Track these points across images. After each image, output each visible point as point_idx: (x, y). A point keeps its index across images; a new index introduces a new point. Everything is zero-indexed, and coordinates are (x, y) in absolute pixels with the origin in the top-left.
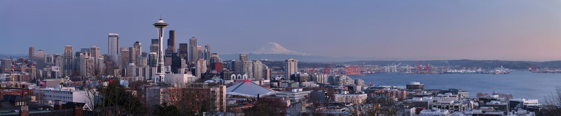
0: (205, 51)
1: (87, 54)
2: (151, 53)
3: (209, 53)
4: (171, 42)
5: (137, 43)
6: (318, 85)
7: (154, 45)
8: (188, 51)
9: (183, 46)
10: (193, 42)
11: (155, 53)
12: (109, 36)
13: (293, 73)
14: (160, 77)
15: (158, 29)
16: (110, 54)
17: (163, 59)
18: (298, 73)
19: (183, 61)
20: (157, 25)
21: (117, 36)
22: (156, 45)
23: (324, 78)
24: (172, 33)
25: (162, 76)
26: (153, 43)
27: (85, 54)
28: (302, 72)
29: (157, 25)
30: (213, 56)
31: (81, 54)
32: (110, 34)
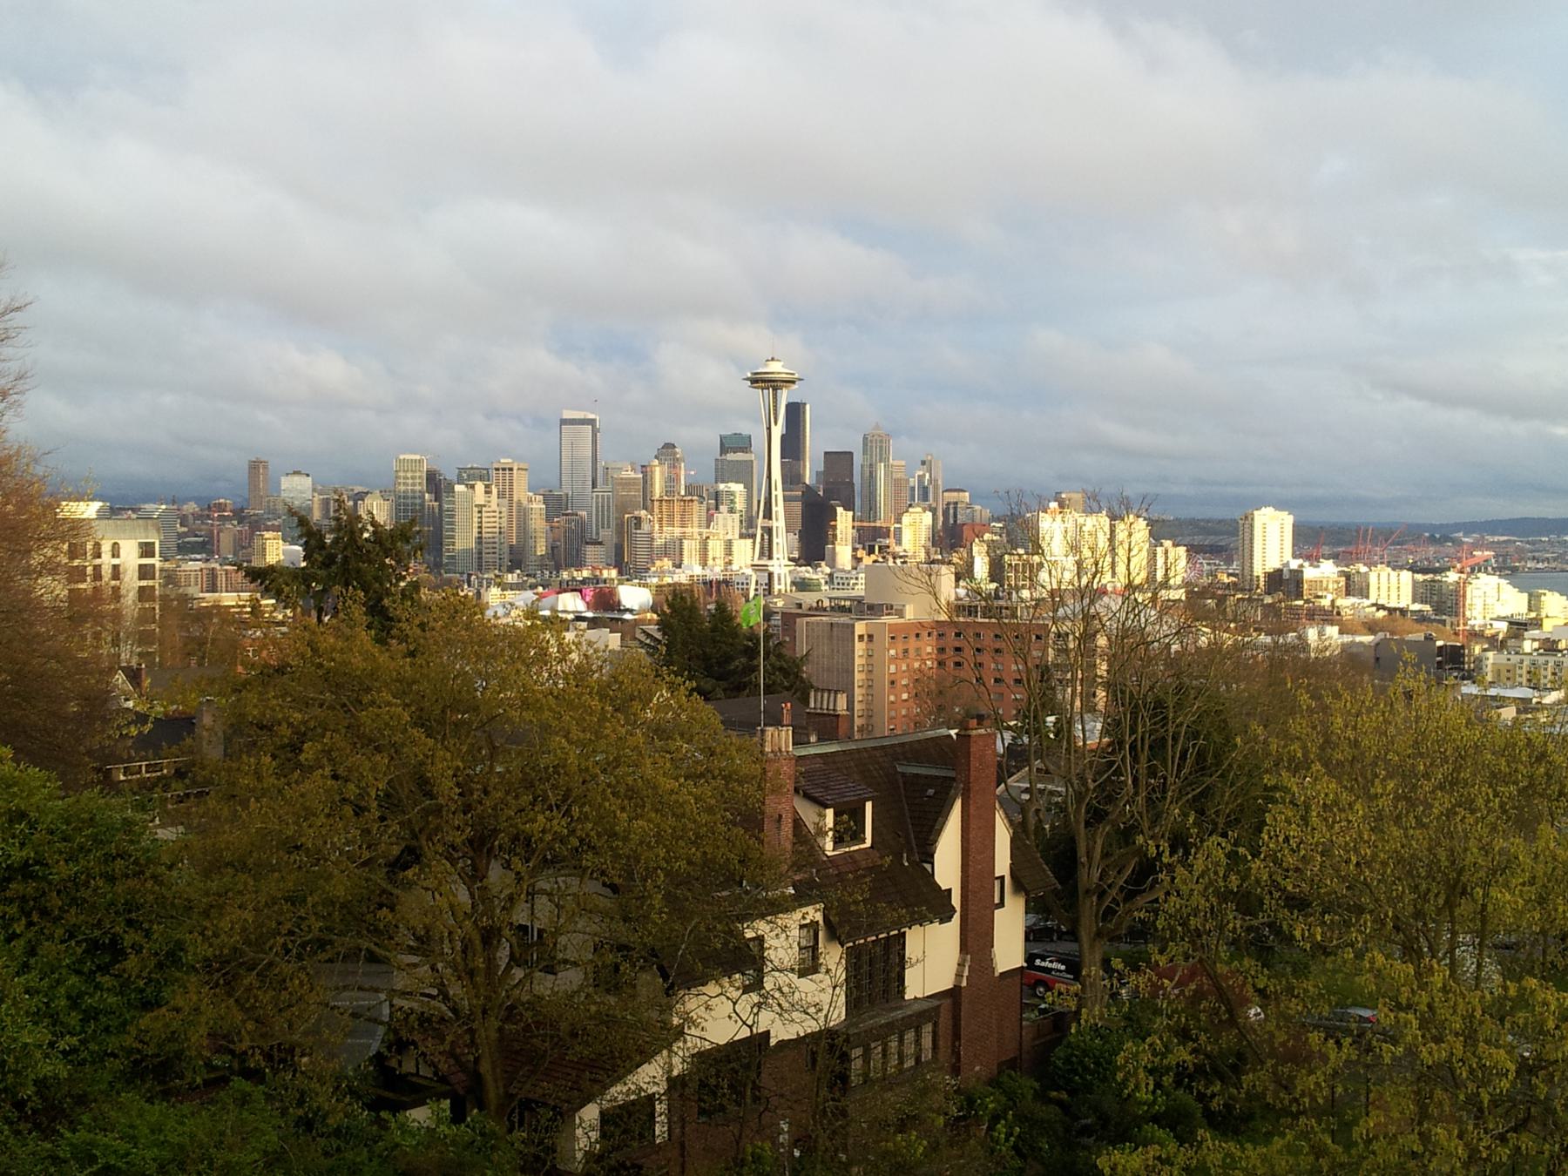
0: (921, 478)
1: (480, 487)
2: (722, 486)
3: (936, 488)
4: (793, 445)
5: (669, 446)
6: (1382, 614)
7: (731, 456)
8: (857, 479)
9: (838, 461)
10: (875, 444)
11: (738, 488)
12: (564, 422)
13: (1273, 564)
14: (770, 575)
15: (760, 396)
16: (566, 490)
17: (779, 508)
18: (1294, 564)
19: (844, 521)
20: (757, 381)
21: (592, 422)
22: (740, 456)
23: (1393, 587)
24: (795, 412)
25: (776, 570)
26: (724, 449)
27: (472, 487)
28: (1314, 559)
29: (757, 381)
30: (952, 497)
31: (459, 488)
32: (567, 415)
